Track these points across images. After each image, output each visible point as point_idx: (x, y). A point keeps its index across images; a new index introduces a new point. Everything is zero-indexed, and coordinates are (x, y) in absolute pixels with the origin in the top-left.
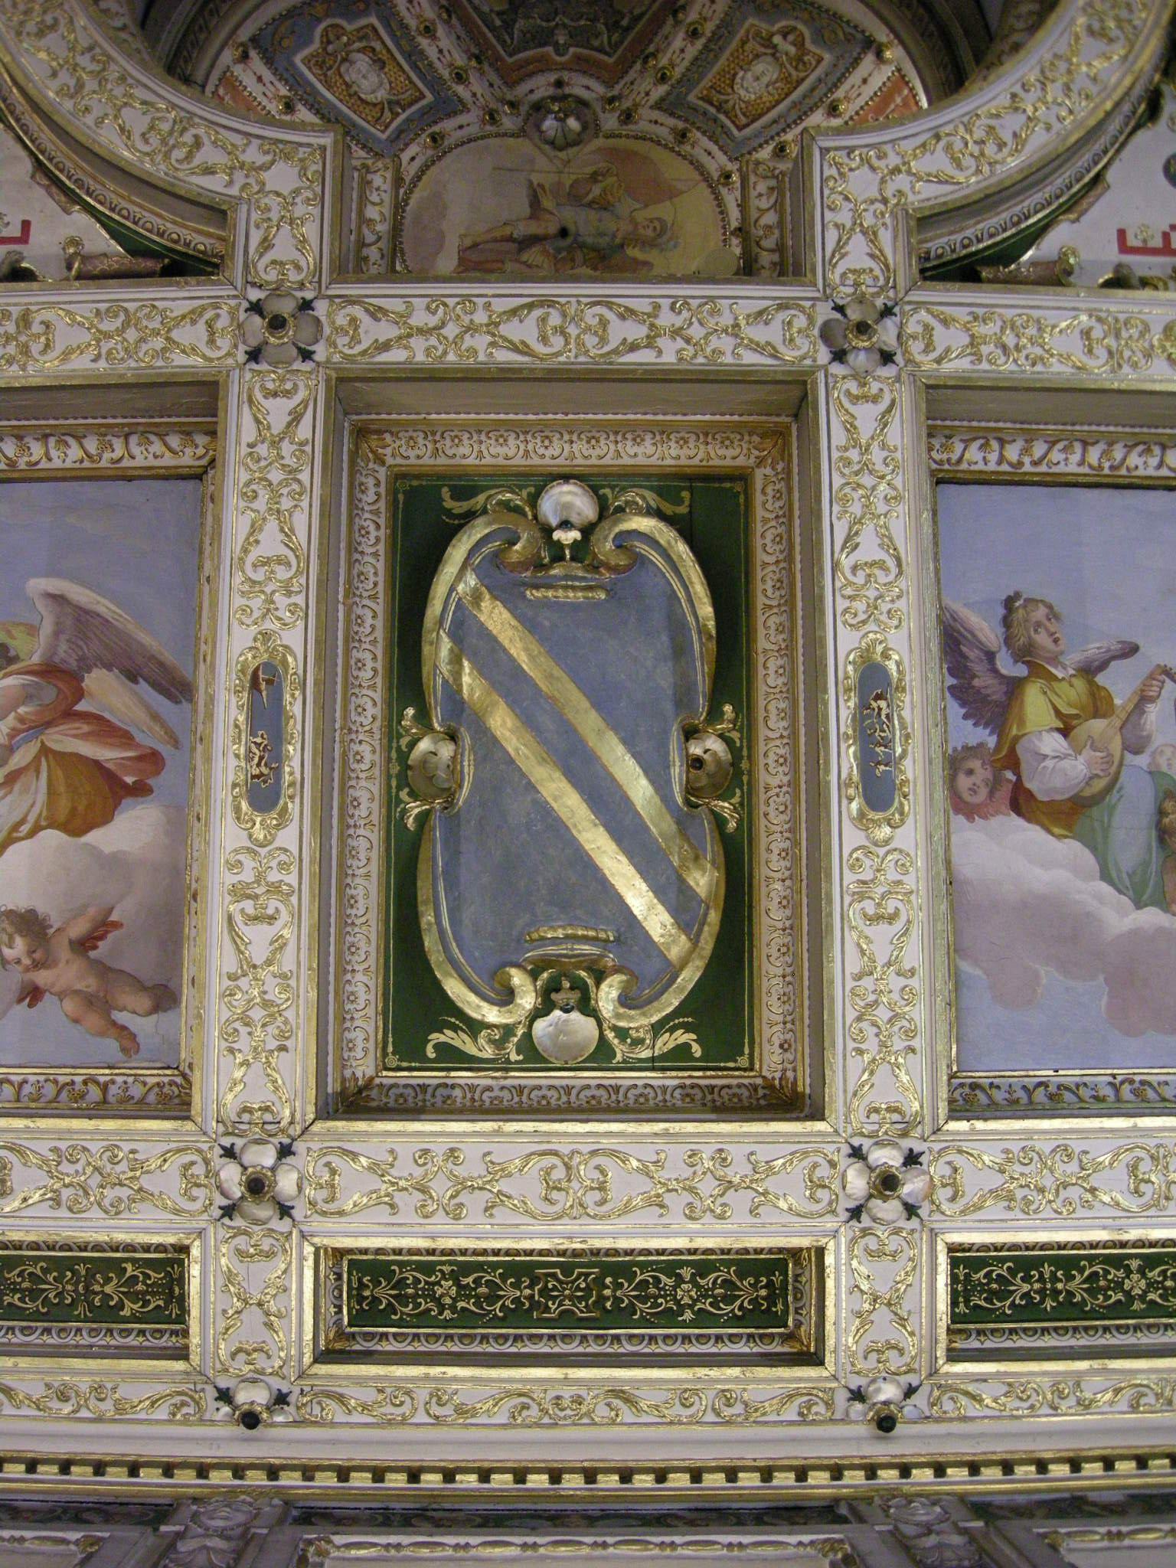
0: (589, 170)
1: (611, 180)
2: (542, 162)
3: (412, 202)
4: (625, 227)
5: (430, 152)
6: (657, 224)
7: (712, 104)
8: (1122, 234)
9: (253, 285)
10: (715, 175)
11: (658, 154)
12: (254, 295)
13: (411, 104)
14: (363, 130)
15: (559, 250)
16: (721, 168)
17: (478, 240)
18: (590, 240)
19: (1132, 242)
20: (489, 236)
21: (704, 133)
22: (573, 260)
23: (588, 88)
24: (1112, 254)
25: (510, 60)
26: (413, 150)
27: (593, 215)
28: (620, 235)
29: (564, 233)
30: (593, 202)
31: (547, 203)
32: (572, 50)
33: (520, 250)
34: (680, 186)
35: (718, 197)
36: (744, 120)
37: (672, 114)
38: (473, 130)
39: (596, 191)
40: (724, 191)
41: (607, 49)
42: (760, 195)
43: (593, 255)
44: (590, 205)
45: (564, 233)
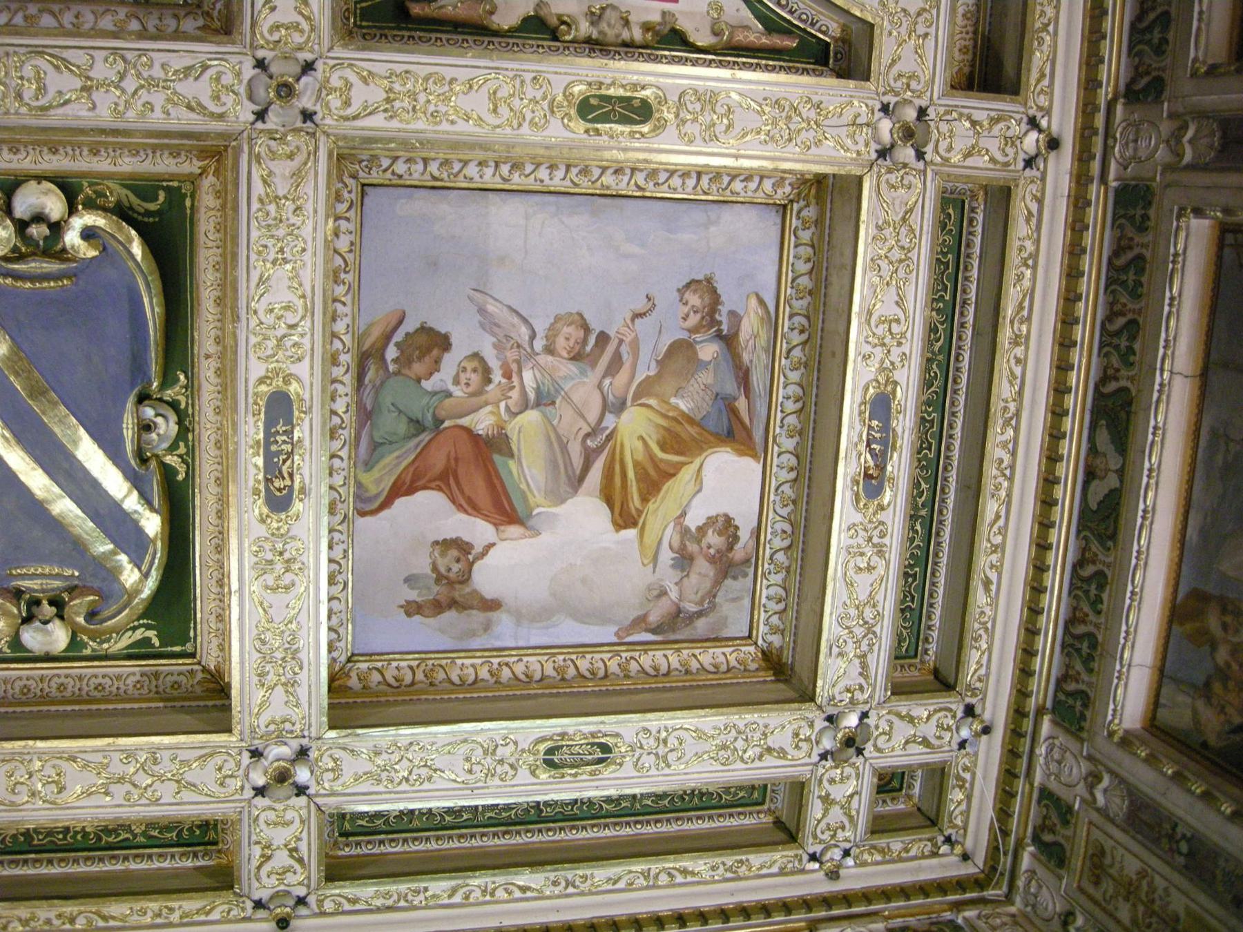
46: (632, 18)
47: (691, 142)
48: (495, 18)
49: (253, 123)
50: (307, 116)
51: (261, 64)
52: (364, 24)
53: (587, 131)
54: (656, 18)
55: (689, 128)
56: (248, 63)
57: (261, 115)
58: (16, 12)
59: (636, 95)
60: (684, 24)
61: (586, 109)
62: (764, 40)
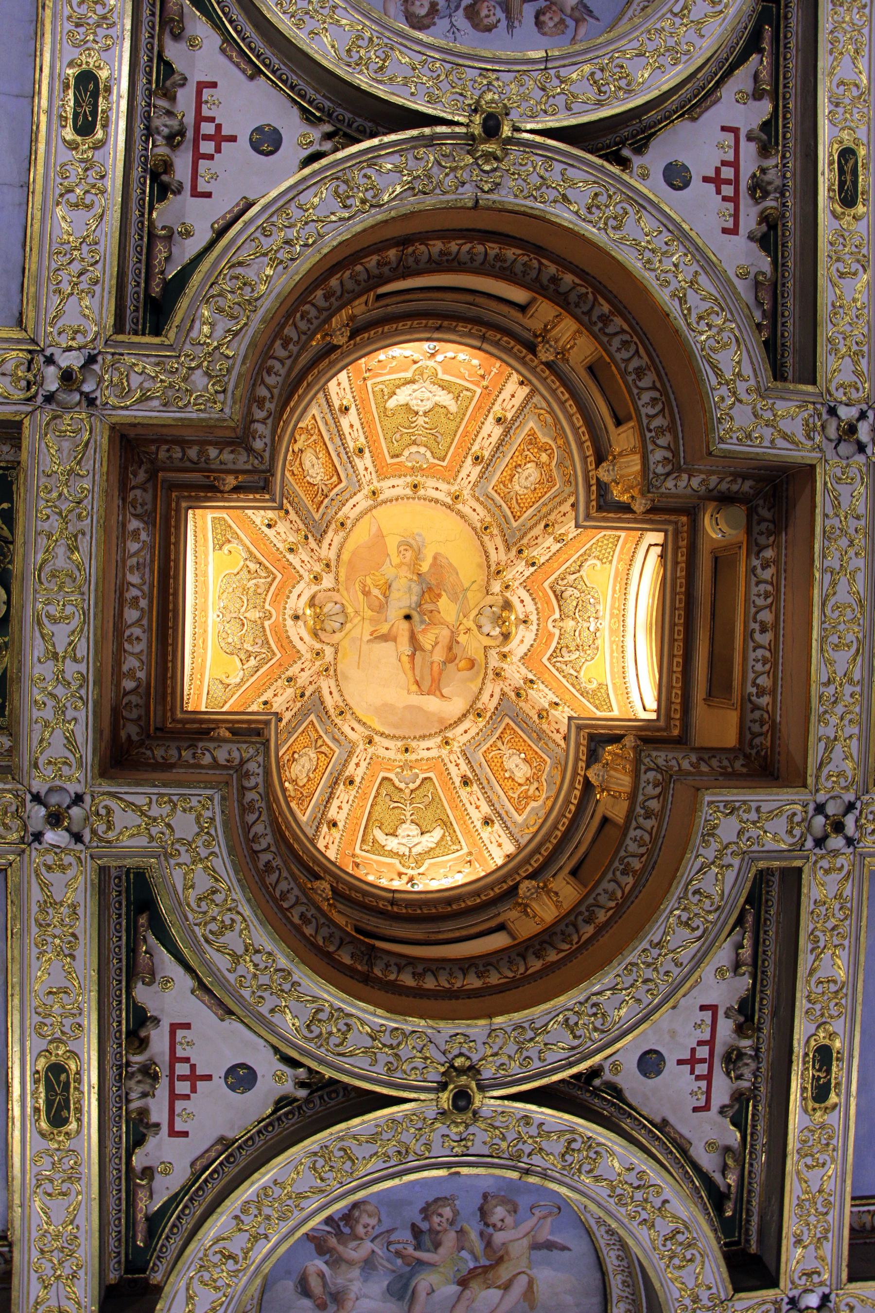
0: (361, 596)
1: (369, 581)
2: (356, 633)
3: (382, 730)
4: (404, 572)
5: (348, 716)
6: (402, 548)
7: (322, 502)
8: (725, 231)
9: (803, 845)
10: (371, 502)
11: (350, 546)
12: (809, 844)
13: (316, 730)
14: (334, 766)
15: (422, 622)
16: (367, 497)
17: (412, 680)
18: (414, 598)
19: (730, 225)
20: (410, 673)
21: (340, 510)
22: (431, 611)
23: (299, 596)
24: (740, 241)
25: (279, 655)
26: (347, 729)
27: (394, 595)
28: (410, 576)
29: (408, 617)
30: (384, 595)
31: (384, 629)
32: (267, 607)
33: (423, 650)
34: (374, 529)
35: (385, 502)
36: (335, 478)
37: (325, 532)
38: (332, 683)
39: (376, 592)
40: (382, 497)
41: (269, 579)
42: (676, 485)
43: (426, 596)
44: (386, 597)
45: (408, 617)
46: (149, 1100)
47: (34, 1162)
48: (140, 985)
49: (30, 792)
50: (38, 837)
51: (78, 799)
52: (132, 876)
53: (37, 1072)
54: (154, 1118)
55: (46, 1161)
56: (80, 789)
57: (37, 798)
58: (142, 590)
59: (72, 1113)
60: (152, 1142)
61: (56, 1069)
62: (140, 1216)
